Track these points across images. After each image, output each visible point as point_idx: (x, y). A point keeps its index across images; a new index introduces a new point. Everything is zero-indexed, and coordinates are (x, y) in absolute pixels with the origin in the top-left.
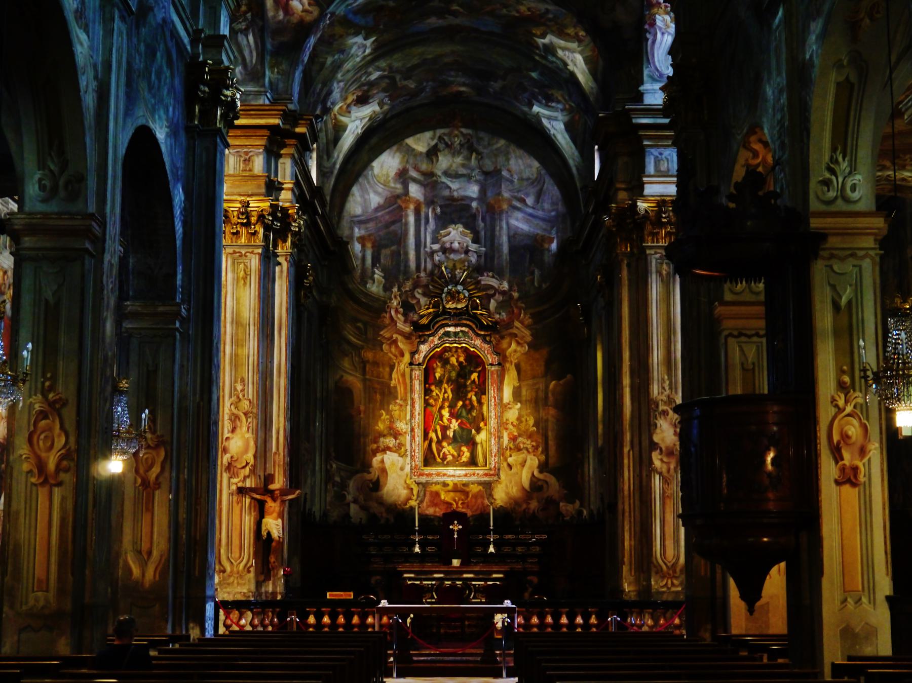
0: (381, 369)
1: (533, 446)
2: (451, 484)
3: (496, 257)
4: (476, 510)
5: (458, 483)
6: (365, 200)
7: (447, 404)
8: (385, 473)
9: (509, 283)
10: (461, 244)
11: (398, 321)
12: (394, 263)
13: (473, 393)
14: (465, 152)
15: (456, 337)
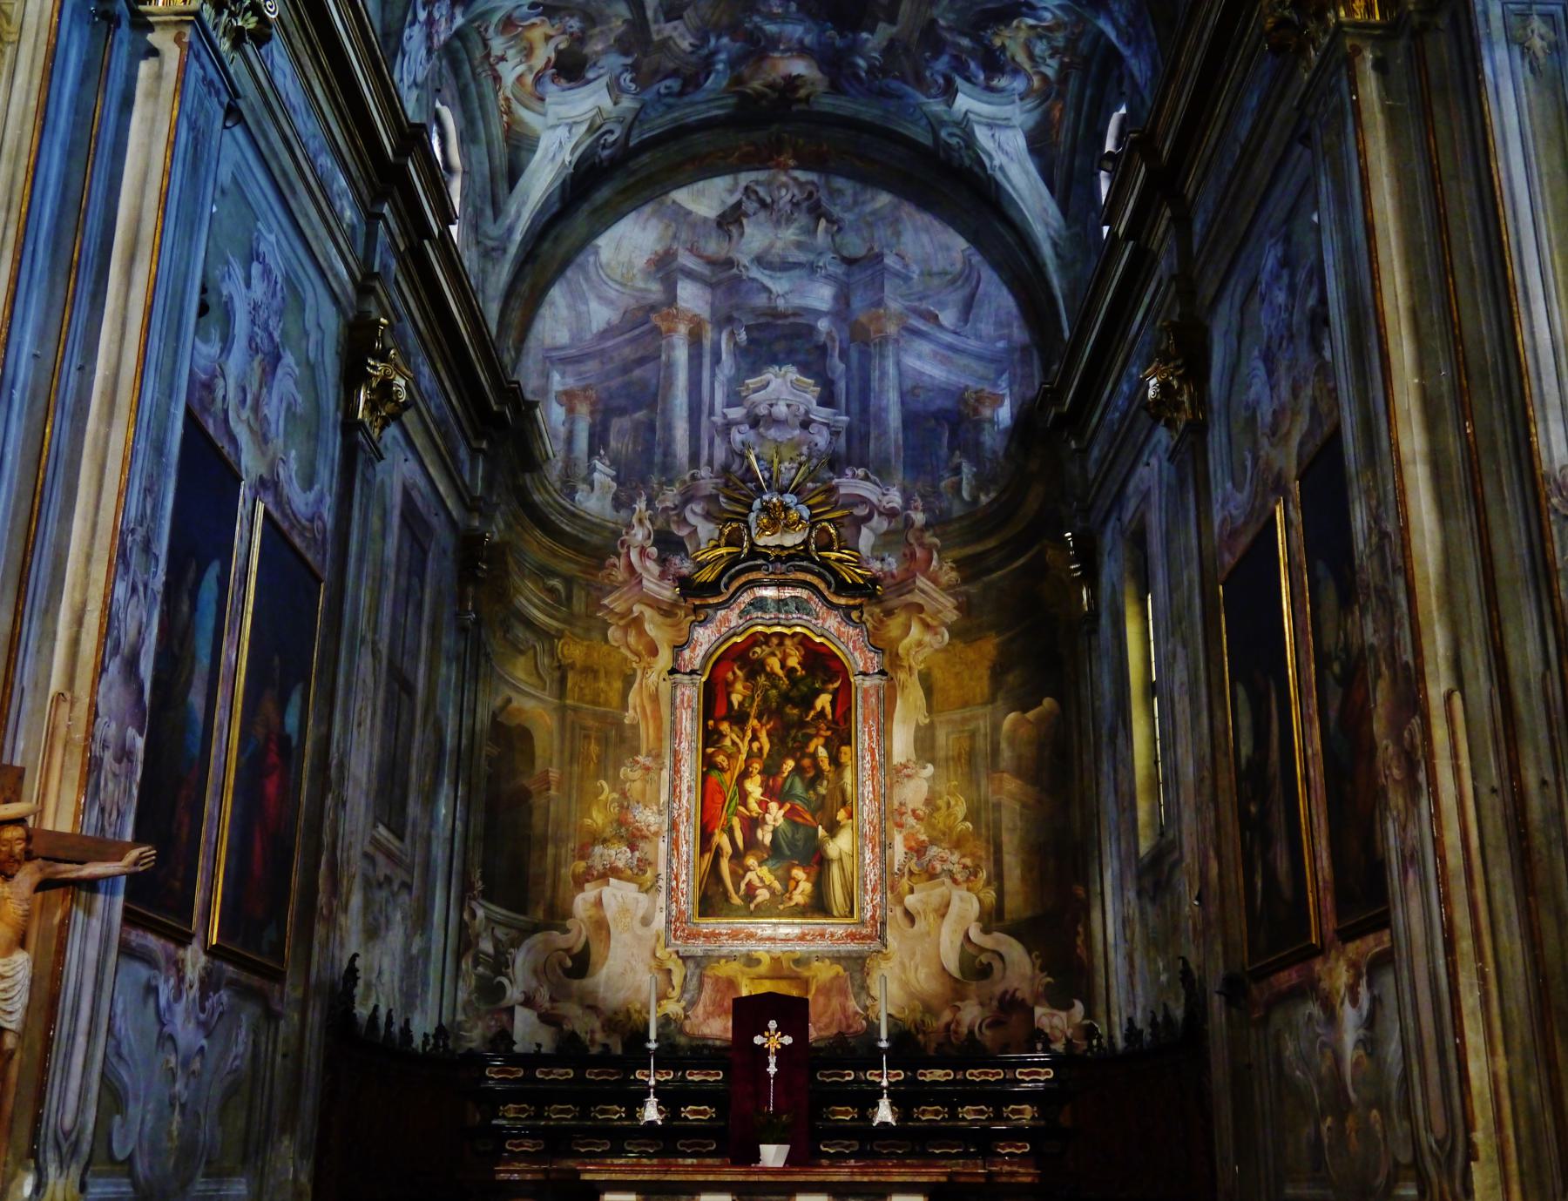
0: (602, 684)
2: (766, 959)
3: (872, 436)
4: (827, 1027)
6: (579, 315)
7: (757, 766)
8: (604, 932)
10: (793, 408)
11: (645, 575)
13: (821, 740)
14: (803, 219)
15: (779, 611)
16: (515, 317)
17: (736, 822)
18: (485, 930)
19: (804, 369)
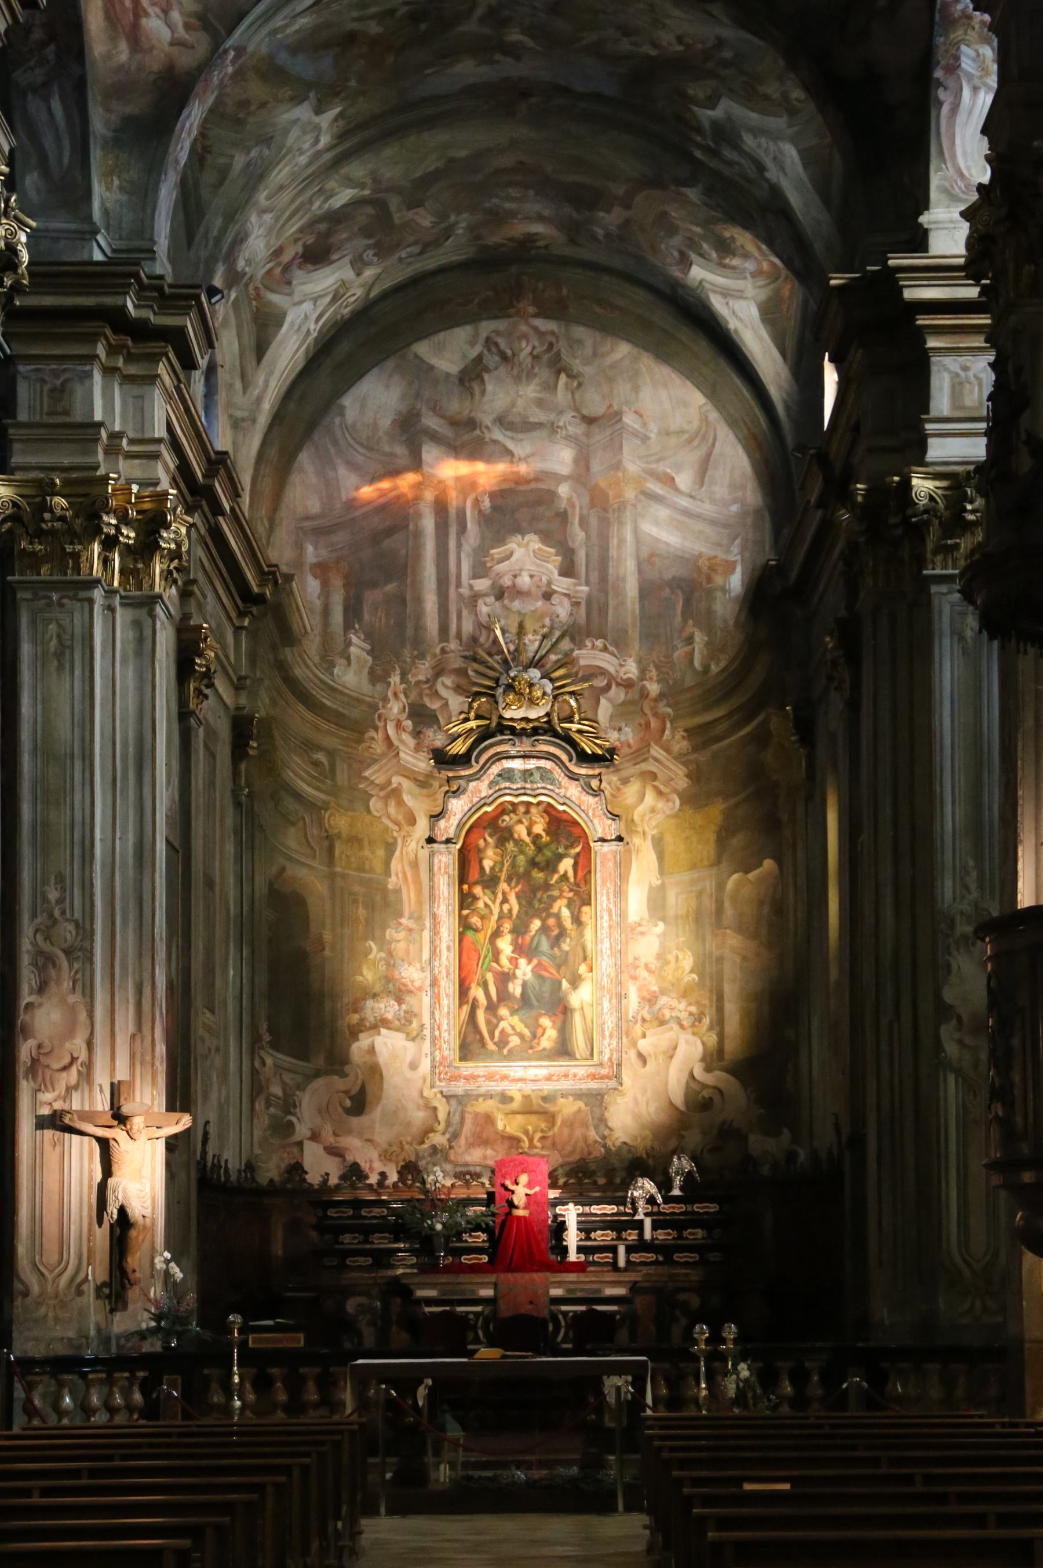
0: (366, 853)
1: (691, 1014)
2: (518, 1097)
3: (611, 606)
5: (533, 1097)
7: (507, 926)
9: (639, 662)
10: (536, 579)
11: (402, 747)
12: (392, 622)
13: (565, 902)
14: (544, 373)
15: (525, 781)
16: (267, 485)
17: (490, 977)
18: (275, 1075)
19: (546, 537)
